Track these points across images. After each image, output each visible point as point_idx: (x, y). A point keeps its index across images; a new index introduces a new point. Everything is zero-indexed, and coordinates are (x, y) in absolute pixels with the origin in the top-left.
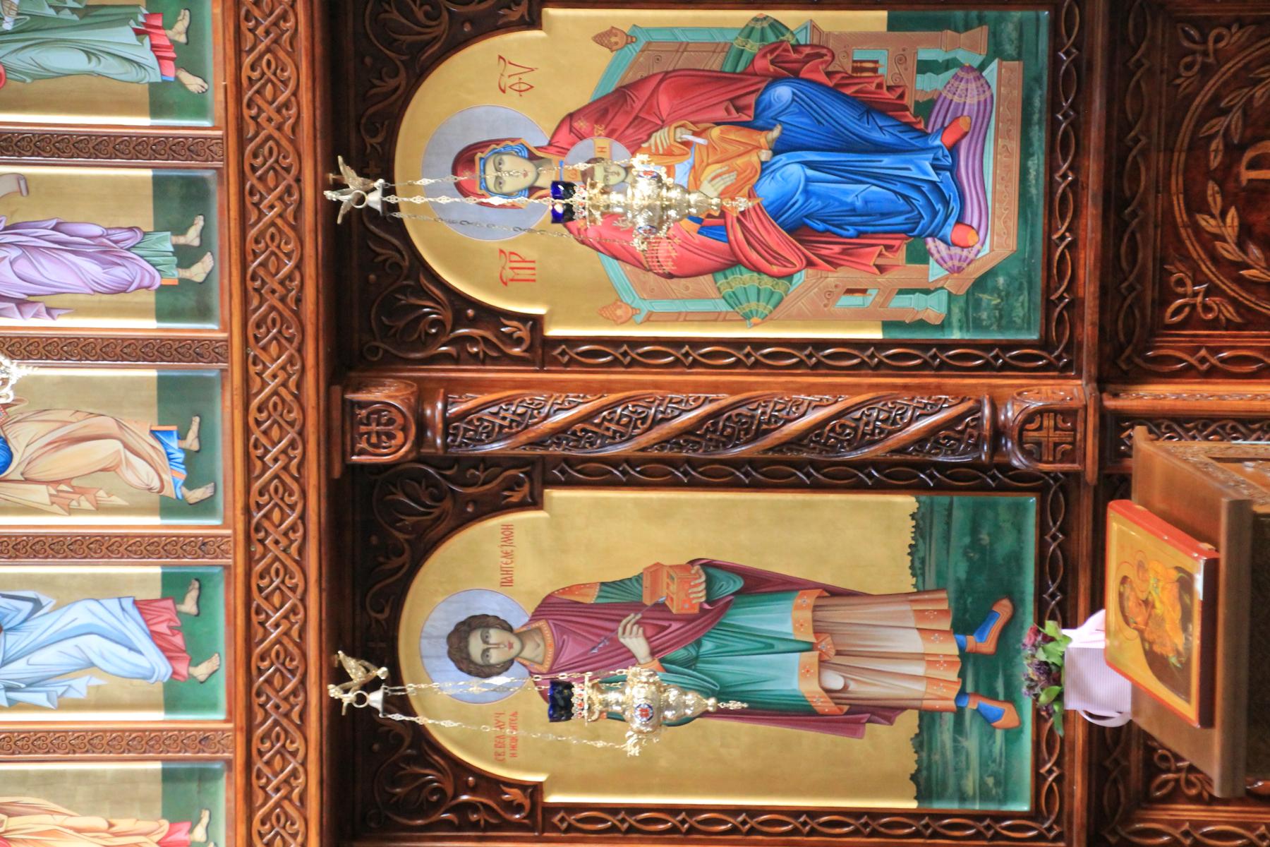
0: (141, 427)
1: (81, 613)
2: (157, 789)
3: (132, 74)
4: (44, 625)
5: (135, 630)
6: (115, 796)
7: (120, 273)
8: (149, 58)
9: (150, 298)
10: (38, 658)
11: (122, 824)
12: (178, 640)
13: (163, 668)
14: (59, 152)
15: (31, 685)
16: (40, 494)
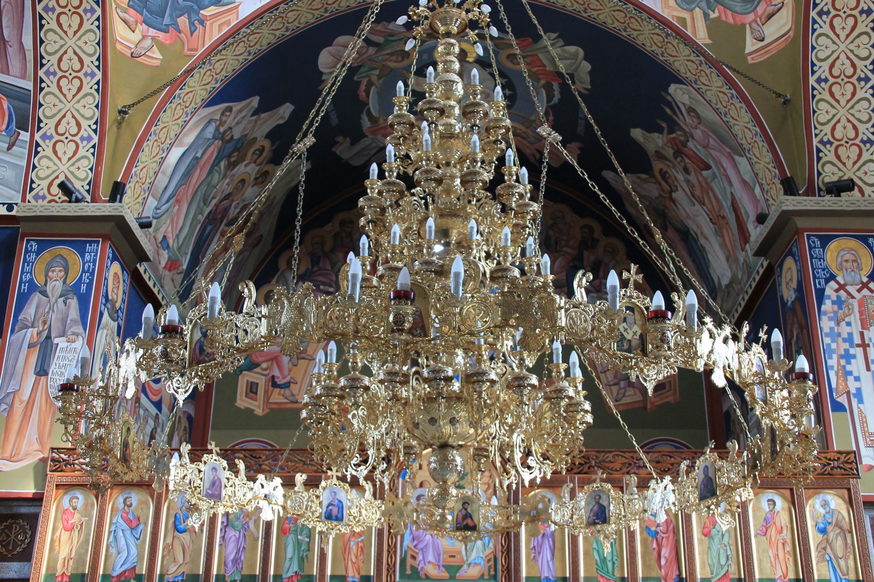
0: (186, 569)
1: (134, 551)
2: (80, 572)
3: (285, 570)
4: (132, 541)
5: (127, 566)
6: (80, 560)
7: (230, 564)
8: (290, 574)
9: (222, 572)
10: (123, 540)
11: (71, 562)
12: (123, 578)
13: (115, 574)
14: (264, 549)
15: (115, 537)
16: (169, 541)
